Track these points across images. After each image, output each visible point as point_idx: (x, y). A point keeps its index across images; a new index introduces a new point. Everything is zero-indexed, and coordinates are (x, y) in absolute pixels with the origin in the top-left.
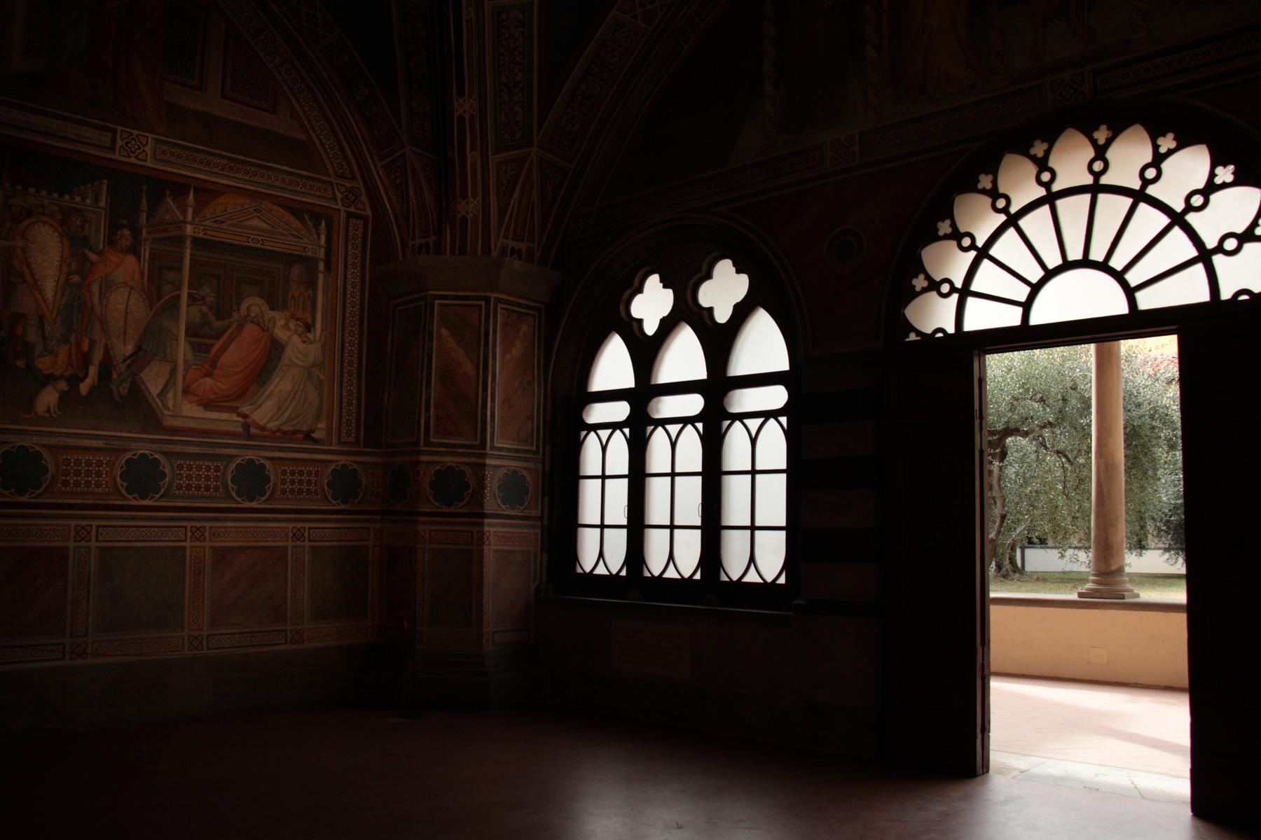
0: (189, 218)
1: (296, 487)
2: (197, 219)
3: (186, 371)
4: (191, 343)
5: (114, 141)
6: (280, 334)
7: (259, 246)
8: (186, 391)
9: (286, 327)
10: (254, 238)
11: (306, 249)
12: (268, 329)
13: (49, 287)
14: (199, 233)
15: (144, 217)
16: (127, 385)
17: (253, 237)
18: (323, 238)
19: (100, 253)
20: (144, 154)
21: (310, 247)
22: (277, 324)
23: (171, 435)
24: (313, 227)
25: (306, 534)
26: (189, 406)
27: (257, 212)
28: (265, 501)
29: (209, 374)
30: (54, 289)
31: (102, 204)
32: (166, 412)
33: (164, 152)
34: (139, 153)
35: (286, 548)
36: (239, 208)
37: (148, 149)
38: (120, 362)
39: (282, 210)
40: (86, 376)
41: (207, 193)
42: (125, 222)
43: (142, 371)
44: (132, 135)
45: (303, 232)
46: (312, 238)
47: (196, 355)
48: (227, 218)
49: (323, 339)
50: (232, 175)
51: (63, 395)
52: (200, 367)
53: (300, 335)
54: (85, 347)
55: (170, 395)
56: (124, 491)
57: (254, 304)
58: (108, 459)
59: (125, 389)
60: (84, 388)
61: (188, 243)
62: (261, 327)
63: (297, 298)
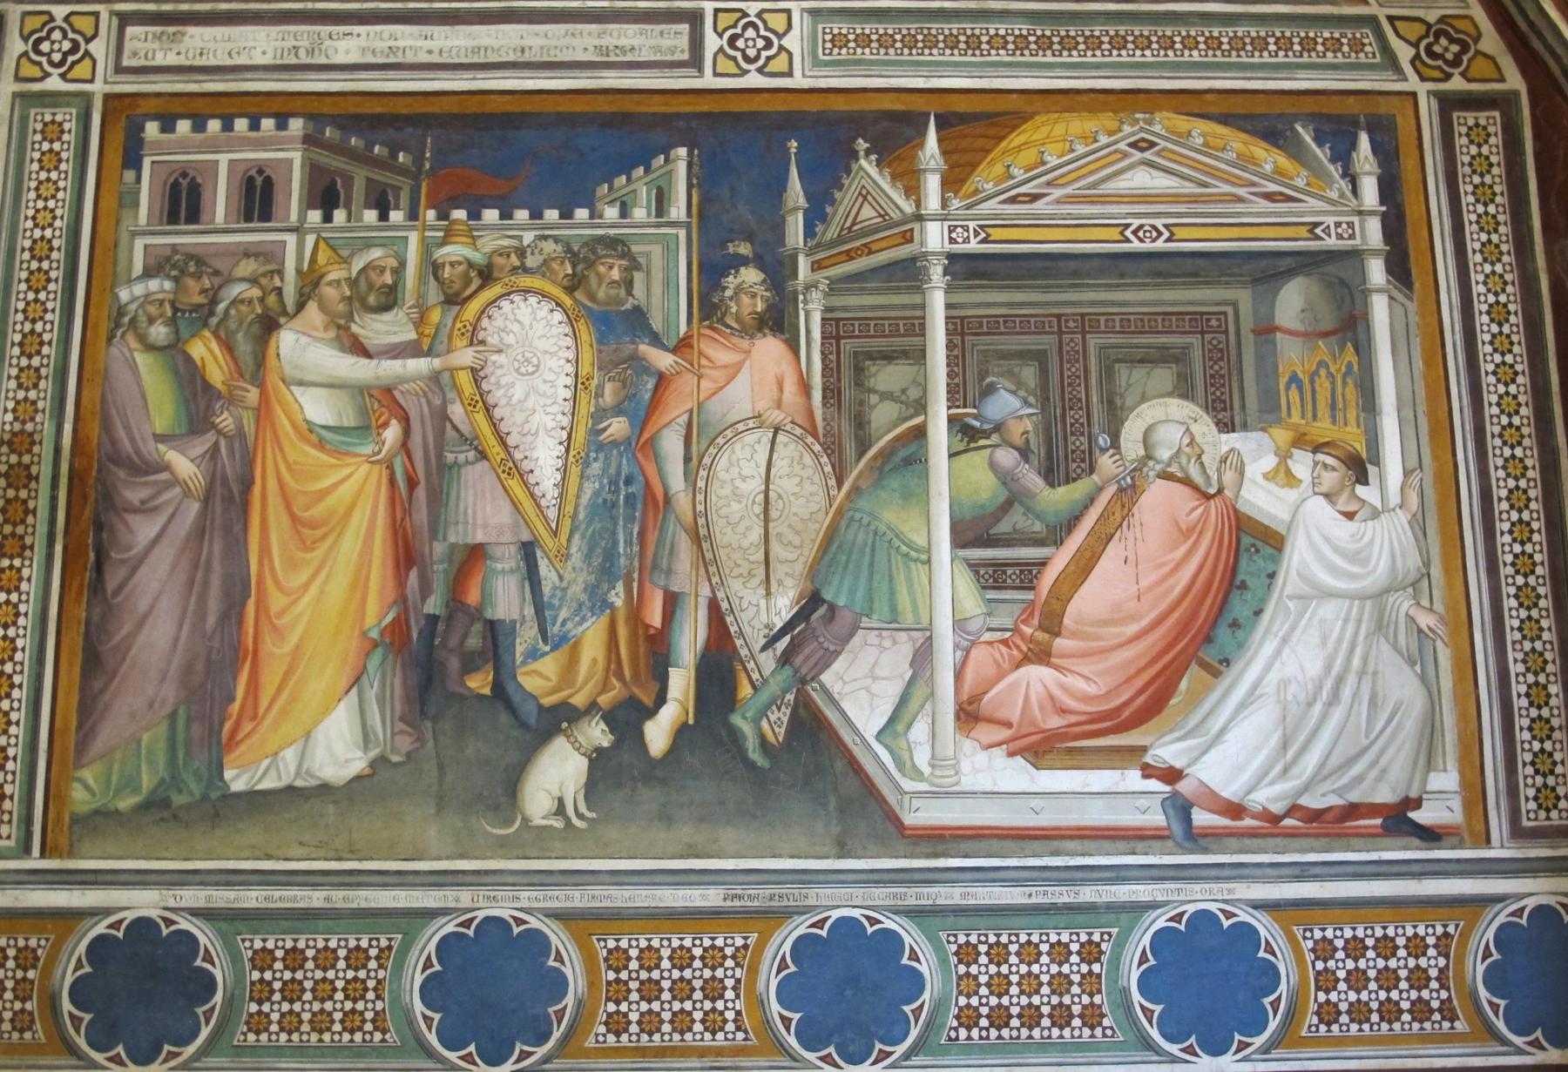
0: (933, 202)
2: (956, 203)
4: (974, 567)
5: (697, 44)
7: (1160, 245)
8: (969, 715)
9: (1283, 475)
10: (1141, 227)
11: (1318, 231)
12: (1220, 491)
14: (967, 240)
15: (795, 228)
16: (781, 716)
19: (682, 346)
20: (784, 55)
22: (1249, 470)
23: (936, 856)
24: (1333, 160)
26: (982, 757)
27: (1142, 150)
29: (1041, 655)
30: (560, 463)
31: (678, 211)
32: (908, 785)
34: (769, 59)
36: (1081, 149)
37: (792, 42)
38: (757, 647)
40: (661, 700)
42: (744, 249)
43: (828, 666)
44: (748, 15)
45: (1300, 183)
46: (1334, 195)
47: (990, 601)
48: (1049, 184)
50: (1050, 59)
51: (598, 760)
52: (1008, 634)
53: (1328, 496)
54: (655, 618)
55: (919, 731)
58: (739, 942)
59: (777, 724)
60: (658, 734)
61: (937, 273)
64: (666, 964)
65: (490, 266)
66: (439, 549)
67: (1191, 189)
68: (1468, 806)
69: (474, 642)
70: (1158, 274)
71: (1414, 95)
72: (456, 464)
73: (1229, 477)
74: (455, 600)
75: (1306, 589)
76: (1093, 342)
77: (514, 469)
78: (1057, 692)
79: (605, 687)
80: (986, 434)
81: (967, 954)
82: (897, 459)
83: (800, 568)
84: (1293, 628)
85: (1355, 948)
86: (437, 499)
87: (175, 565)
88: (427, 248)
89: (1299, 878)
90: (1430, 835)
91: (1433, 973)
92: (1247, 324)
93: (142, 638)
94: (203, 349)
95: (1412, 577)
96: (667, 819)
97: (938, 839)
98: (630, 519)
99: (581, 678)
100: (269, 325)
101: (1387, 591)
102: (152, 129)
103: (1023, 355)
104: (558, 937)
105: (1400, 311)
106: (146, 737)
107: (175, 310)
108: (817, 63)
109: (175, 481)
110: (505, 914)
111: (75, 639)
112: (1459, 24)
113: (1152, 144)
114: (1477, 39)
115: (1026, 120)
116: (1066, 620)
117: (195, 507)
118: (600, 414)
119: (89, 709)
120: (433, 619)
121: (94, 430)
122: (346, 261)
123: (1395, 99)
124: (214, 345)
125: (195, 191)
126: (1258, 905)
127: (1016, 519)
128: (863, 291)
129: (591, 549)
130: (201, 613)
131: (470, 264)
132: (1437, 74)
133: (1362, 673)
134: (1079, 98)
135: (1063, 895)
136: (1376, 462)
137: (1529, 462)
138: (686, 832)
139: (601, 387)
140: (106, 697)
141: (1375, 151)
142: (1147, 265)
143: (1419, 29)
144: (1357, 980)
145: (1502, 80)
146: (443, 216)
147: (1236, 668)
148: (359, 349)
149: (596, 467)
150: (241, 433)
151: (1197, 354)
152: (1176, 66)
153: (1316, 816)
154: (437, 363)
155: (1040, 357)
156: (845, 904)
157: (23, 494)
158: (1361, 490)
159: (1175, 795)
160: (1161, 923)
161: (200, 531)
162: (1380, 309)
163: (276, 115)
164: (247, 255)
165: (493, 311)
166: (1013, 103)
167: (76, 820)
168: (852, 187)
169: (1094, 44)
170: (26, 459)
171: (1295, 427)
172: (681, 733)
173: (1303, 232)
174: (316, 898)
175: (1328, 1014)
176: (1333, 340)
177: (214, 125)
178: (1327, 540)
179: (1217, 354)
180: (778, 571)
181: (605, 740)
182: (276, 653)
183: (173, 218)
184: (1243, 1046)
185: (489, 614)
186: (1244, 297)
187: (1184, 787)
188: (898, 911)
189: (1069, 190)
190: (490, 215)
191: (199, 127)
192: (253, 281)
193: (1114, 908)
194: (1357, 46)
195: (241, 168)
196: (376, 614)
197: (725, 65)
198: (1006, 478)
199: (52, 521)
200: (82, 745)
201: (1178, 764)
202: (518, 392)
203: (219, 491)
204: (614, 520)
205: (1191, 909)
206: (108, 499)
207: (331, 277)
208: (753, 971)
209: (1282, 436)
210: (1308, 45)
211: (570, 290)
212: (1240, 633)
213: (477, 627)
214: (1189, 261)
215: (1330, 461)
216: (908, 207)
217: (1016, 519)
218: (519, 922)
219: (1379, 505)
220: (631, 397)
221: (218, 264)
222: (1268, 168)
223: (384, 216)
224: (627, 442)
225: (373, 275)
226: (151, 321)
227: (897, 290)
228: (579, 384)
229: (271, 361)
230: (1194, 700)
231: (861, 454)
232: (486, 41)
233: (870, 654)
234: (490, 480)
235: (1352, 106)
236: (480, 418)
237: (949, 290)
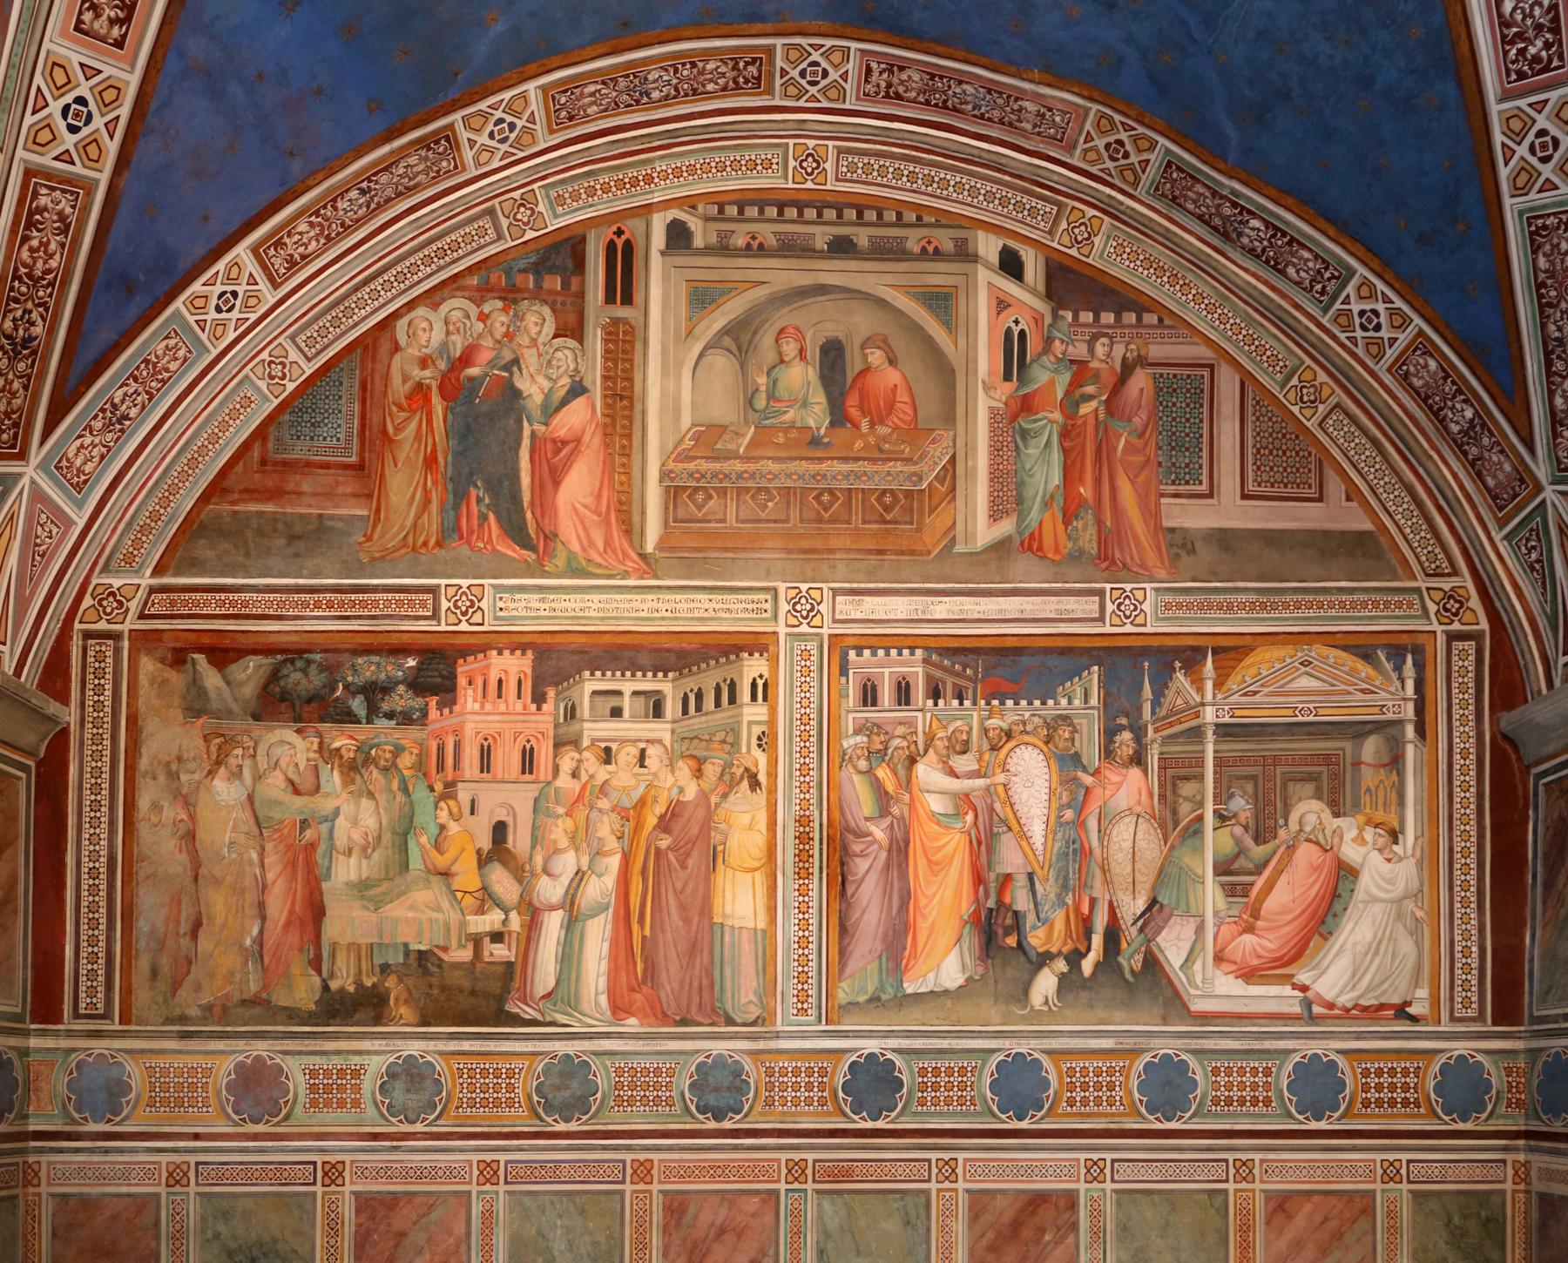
0: (1209, 697)
1: (1385, 1095)
2: (1219, 696)
3: (1218, 926)
4: (1222, 885)
6: (1350, 852)
7: (1311, 718)
13: (1037, 831)
15: (1147, 708)
16: (1139, 958)
17: (1301, 706)
18: (1410, 685)
21: (1390, 704)
24: (1394, 670)
25: (1403, 1172)
26: (1224, 979)
28: (1339, 1119)
31: (1094, 701)
32: (1193, 992)
33: (1168, 606)
35: (1374, 1192)
36: (1278, 666)
37: (1146, 607)
39: (1344, 654)
40: (1089, 950)
41: (1230, 652)
42: (1124, 721)
43: (1159, 933)
45: (1377, 683)
48: (1262, 685)
49: (1418, 853)
51: (1062, 978)
53: (1380, 850)
54: (1086, 910)
55: (1198, 966)
56: (1143, 1110)
57: (1309, 811)
59: (1139, 958)
60: (1087, 966)
62: (1321, 846)
63: (1373, 789)
64: (1091, 1075)
65: (1010, 730)
66: (993, 876)
67: (1328, 687)
68: (1432, 1004)
69: (1009, 921)
70: (1309, 734)
71: (1435, 632)
72: (998, 833)
73: (1336, 840)
74: (1000, 902)
75: (1367, 898)
76: (1279, 770)
77: (1023, 836)
78: (1257, 947)
79: (1065, 943)
80: (1229, 819)
81: (1216, 1071)
82: (1191, 831)
83: (1148, 886)
84: (1360, 917)
85: (1379, 1073)
86: (990, 851)
87: (878, 881)
88: (982, 722)
89: (1358, 1039)
90: (1414, 1019)
91: (1412, 1085)
92: (1349, 760)
93: (865, 918)
94: (883, 773)
95: (1416, 891)
96: (1091, 1006)
97: (1205, 1017)
98: (1075, 861)
99: (1055, 939)
100: (912, 761)
101: (1403, 898)
102: (852, 653)
103: (1246, 777)
104: (1046, 1062)
105: (1419, 754)
106: (869, 967)
107: (869, 752)
108: (1158, 619)
109: (875, 841)
110: (1024, 1051)
111: (835, 919)
112: (1461, 591)
113: (1311, 663)
114: (1468, 600)
115: (1253, 650)
116: (1262, 913)
117: (884, 855)
118: (1061, 808)
119: (843, 953)
120: (991, 910)
121: (836, 814)
122: (945, 727)
123: (1425, 635)
124: (888, 771)
125: (874, 688)
126: (1339, 1052)
127: (1241, 863)
128: (1177, 744)
129: (1058, 876)
130: (890, 907)
131: (1002, 730)
132: (1447, 621)
133: (1390, 939)
134: (1278, 637)
135: (1256, 1045)
136: (1403, 832)
137: (1472, 833)
138: (1100, 1013)
139: (1061, 794)
140: (851, 948)
141: (1414, 665)
142: (1305, 729)
143: (1441, 594)
144: (1379, 1088)
145: (1478, 624)
146: (988, 704)
147: (1333, 938)
148: (953, 774)
149: (1059, 835)
150: (903, 818)
151: (1325, 777)
152: (1323, 618)
153: (1365, 1009)
154: (988, 781)
155: (1254, 778)
156: (1165, 1047)
157: (807, 847)
158: (1395, 847)
159: (1305, 998)
160: (1297, 1059)
161: (887, 866)
162: (1410, 751)
163: (910, 648)
164: (900, 724)
165: (1012, 754)
166: (1248, 640)
167: (840, 1007)
168: (1173, 686)
169: (1286, 606)
170: (807, 829)
171: (1366, 815)
172: (1097, 966)
173: (1376, 710)
174: (944, 1044)
175: (1366, 1103)
176: (1387, 768)
177: (881, 652)
178: (1379, 873)
179: (1335, 776)
180: (1139, 886)
181: (1065, 969)
182: (924, 926)
183: (865, 704)
184: (1330, 1117)
185: (1015, 908)
186: (1348, 745)
187: (1310, 994)
188: (1187, 1051)
189: (1271, 689)
190: (1010, 703)
191: (874, 654)
192: (904, 737)
193: (1276, 1051)
194: (1411, 605)
195: (895, 676)
196: (966, 909)
197: (1116, 621)
198: (1238, 841)
199: (821, 861)
200: (842, 970)
201: (1307, 983)
202: (1024, 797)
203: (894, 846)
204: (1067, 861)
205: (1310, 1052)
206: (845, 849)
207: (939, 736)
208: (1127, 1078)
209: (1361, 819)
210: (1387, 604)
211: (1047, 743)
212: (1337, 920)
213: (1010, 914)
214: (1323, 727)
215: (1382, 832)
216: (1198, 699)
217: (1241, 863)
218: (1030, 1055)
219: (1402, 854)
220: (1074, 799)
221: (889, 728)
222: (1363, 675)
223: (961, 704)
224: (1073, 822)
225: (957, 734)
226: (859, 758)
227: (1192, 743)
228: (1051, 792)
229: (914, 780)
230: (1318, 950)
231: (1175, 829)
232: (1004, 607)
233: (1178, 927)
234: (1013, 842)
235: (1405, 639)
236: (1008, 809)
237: (1216, 743)
